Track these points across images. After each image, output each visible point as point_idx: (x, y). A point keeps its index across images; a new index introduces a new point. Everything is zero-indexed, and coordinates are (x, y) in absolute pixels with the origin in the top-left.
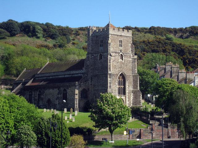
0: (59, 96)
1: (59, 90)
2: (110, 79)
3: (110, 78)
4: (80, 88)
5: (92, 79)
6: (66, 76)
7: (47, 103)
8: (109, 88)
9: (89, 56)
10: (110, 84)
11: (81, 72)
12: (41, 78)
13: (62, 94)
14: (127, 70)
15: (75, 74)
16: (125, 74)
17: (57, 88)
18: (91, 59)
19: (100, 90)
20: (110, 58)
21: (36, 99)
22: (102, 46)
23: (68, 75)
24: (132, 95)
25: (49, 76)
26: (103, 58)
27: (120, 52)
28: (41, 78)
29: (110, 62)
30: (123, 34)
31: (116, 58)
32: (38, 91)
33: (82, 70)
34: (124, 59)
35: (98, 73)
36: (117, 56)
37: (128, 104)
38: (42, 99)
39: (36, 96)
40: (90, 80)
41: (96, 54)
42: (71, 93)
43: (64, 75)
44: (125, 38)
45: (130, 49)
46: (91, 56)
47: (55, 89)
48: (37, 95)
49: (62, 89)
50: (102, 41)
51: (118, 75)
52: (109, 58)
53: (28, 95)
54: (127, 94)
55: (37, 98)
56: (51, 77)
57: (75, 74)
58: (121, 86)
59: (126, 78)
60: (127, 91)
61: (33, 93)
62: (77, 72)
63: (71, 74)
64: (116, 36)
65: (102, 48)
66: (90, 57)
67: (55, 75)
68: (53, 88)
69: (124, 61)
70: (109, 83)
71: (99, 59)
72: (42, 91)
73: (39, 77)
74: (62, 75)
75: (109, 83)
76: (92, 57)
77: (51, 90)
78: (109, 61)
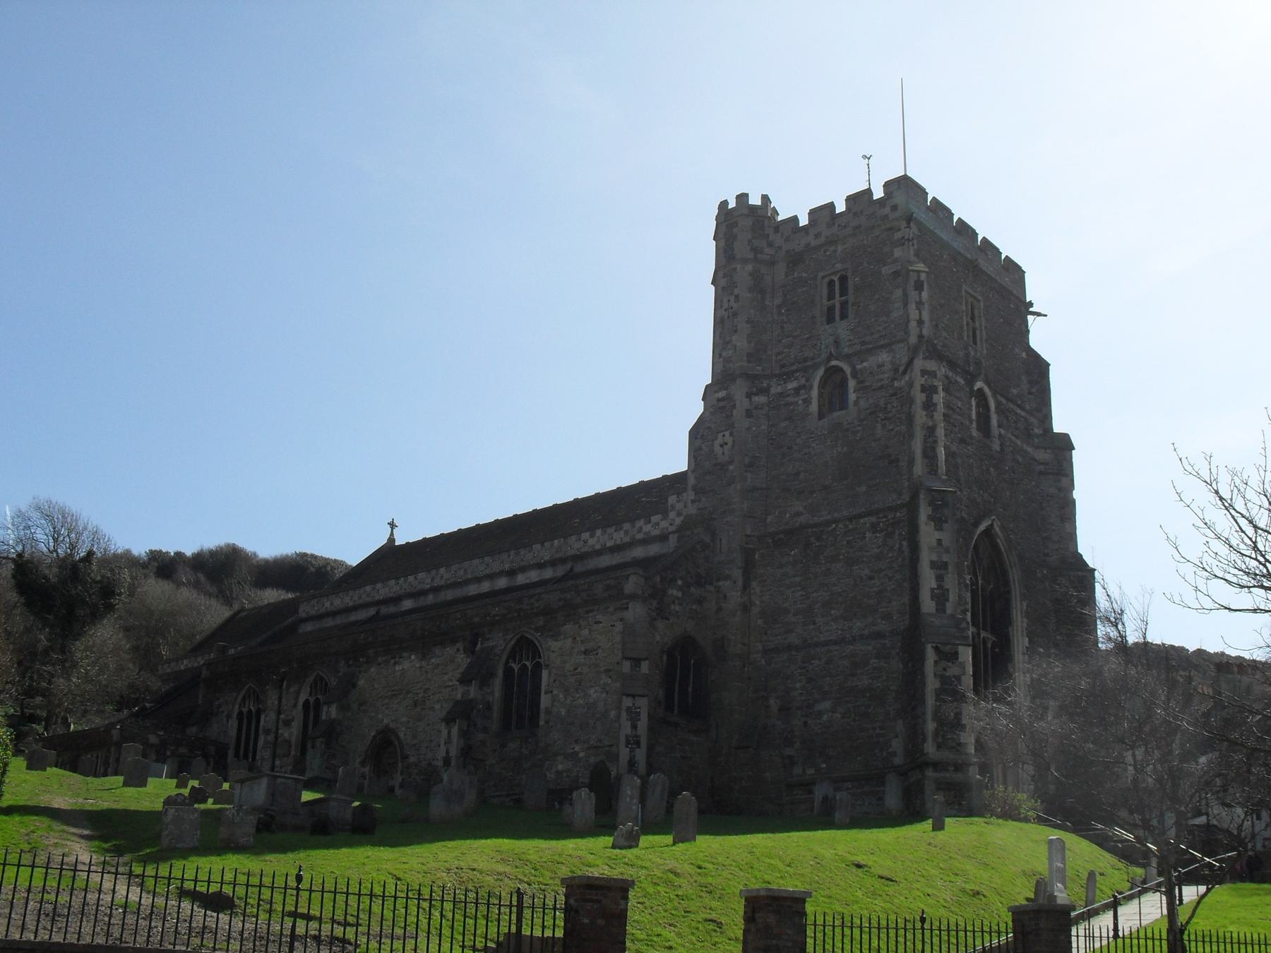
0: (473, 692)
1: (470, 651)
2: (937, 535)
5: (748, 567)
6: (521, 579)
7: (363, 763)
9: (728, 398)
10: (940, 578)
11: (647, 528)
12: (339, 620)
13: (498, 683)
15: (599, 553)
17: (454, 641)
18: (749, 414)
19: (827, 643)
20: (932, 374)
21: (288, 742)
22: (844, 316)
23: (540, 566)
25: (397, 600)
26: (852, 396)
28: (339, 620)
29: (929, 406)
32: (311, 679)
33: (665, 514)
35: (802, 519)
38: (332, 733)
39: (288, 723)
40: (737, 573)
41: (788, 376)
42: (581, 659)
43: (511, 573)
46: (749, 395)
47: (437, 651)
48: (298, 713)
49: (499, 642)
50: (843, 280)
52: (924, 372)
53: (233, 723)
55: (292, 733)
56: (408, 604)
57: (599, 553)
58: (983, 634)
61: (272, 699)
62: (618, 537)
63: (563, 561)
65: (842, 329)
66: (742, 403)
67: (438, 582)
68: (424, 643)
69: (996, 446)
70: (933, 565)
71: (814, 407)
72: (333, 682)
73: (320, 617)
74: (491, 577)
76: (761, 399)
77: (409, 665)
78: (920, 397)
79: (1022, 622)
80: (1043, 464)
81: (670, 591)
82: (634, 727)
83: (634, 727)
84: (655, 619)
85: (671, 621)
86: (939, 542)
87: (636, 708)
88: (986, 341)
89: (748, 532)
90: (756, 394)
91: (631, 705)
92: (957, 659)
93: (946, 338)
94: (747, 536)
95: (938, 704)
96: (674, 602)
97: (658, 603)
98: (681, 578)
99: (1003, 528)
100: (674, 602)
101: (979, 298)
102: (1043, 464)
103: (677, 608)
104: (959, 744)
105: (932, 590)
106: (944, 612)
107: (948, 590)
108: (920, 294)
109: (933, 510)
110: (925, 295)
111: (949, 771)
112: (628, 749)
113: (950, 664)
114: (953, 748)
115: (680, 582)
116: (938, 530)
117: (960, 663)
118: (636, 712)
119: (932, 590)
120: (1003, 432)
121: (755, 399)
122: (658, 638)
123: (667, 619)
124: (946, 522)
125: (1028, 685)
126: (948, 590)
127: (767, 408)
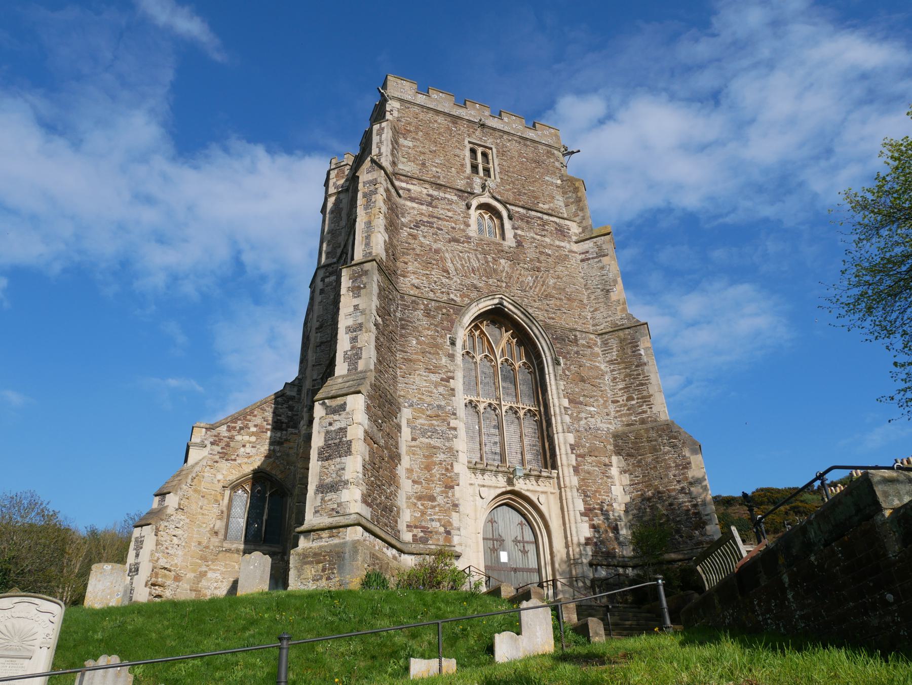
2: (356, 301)
3: (356, 290)
4: (224, 465)
8: (341, 368)
10: (354, 339)
14: (548, 296)
16: (526, 314)
24: (614, 471)
27: (478, 190)
30: (493, 123)
31: (439, 212)
34: (509, 233)
36: (451, 202)
37: (588, 541)
44: (513, 147)
45: (561, 199)
51: (460, 310)
54: (565, 457)
59: (543, 345)
60: (563, 440)
64: (440, 119)
69: (510, 241)
75: (349, 329)
79: (557, 384)
80: (583, 253)
81: (238, 438)
82: (137, 555)
83: (137, 555)
84: (217, 462)
85: (239, 461)
86: (356, 307)
87: (141, 537)
88: (500, 173)
89: (315, 377)
90: (329, 277)
91: (139, 535)
92: (344, 410)
93: (437, 172)
94: (313, 380)
95: (320, 463)
96: (244, 446)
97: (222, 448)
98: (256, 426)
99: (515, 304)
100: (244, 446)
101: (493, 147)
102: (583, 253)
103: (248, 449)
104: (339, 505)
105: (346, 353)
106: (356, 369)
107: (361, 348)
108: (381, 136)
109: (353, 282)
110: (384, 136)
111: (321, 538)
112: (130, 578)
113: (336, 417)
114: (333, 509)
115: (253, 429)
116: (355, 297)
117: (348, 413)
118: (141, 541)
119: (346, 353)
120: (519, 232)
121: (327, 280)
122: (220, 477)
123: (235, 460)
124: (365, 287)
125: (571, 445)
126: (361, 348)
127: (334, 284)
